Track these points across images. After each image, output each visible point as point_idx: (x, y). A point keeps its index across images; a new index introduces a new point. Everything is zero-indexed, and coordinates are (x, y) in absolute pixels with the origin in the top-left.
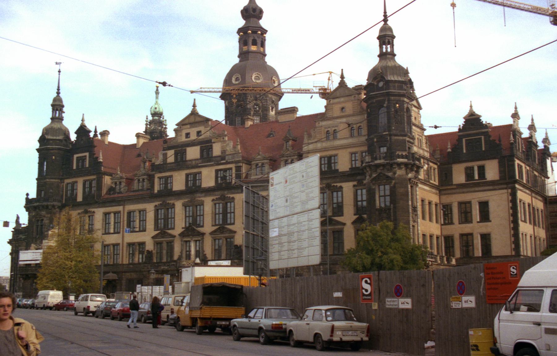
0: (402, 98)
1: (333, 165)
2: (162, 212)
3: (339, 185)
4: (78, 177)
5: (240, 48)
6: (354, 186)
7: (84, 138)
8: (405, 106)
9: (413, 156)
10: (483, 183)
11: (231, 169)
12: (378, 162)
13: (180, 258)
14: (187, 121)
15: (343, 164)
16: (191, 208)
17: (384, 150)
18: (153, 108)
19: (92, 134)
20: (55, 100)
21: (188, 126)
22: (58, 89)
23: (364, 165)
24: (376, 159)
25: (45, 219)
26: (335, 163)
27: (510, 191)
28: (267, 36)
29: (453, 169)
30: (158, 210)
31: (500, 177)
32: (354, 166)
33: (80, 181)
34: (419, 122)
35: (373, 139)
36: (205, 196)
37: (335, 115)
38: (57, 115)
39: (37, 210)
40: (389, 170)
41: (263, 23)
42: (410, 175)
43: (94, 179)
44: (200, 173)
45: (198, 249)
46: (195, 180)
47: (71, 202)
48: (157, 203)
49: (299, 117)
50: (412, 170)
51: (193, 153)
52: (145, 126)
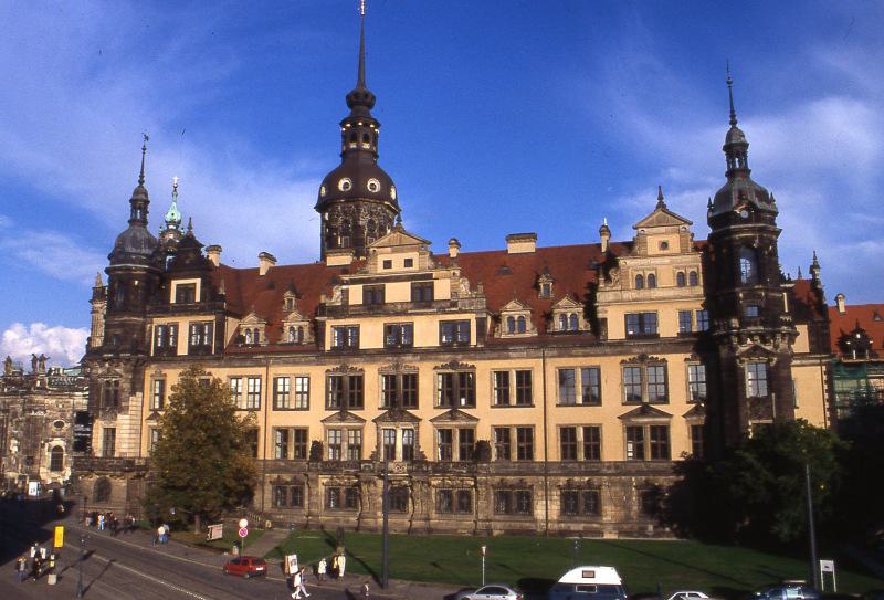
3: (660, 357)
4: (180, 316)
6: (686, 360)
11: (468, 322)
13: (375, 456)
20: (137, 192)
22: (142, 176)
25: (122, 381)
27: (824, 368)
31: (811, 350)
33: (184, 324)
36: (422, 360)
37: (649, 253)
41: (373, 113)
43: (210, 323)
45: (406, 442)
48: (330, 367)
51: (397, 293)
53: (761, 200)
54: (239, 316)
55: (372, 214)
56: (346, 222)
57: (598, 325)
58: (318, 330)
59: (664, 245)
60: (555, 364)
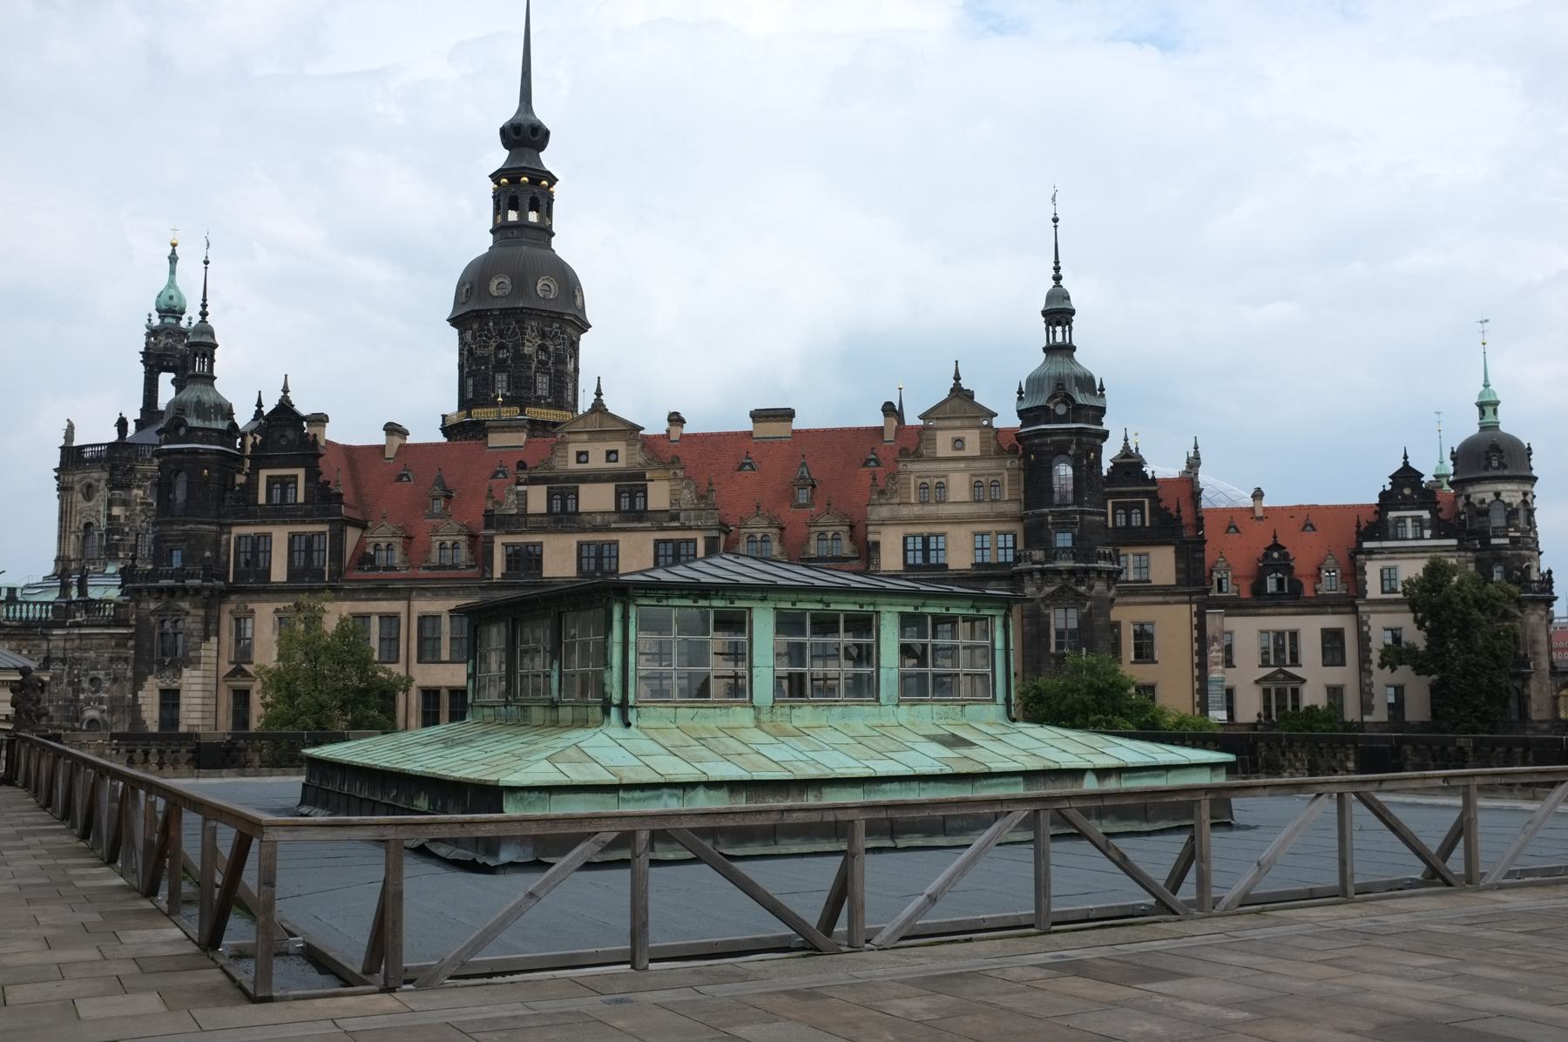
1: (933, 554)
4: (273, 523)
15: (959, 553)
17: (1064, 540)
18: (165, 298)
21: (585, 437)
23: (1022, 566)
27: (1195, 608)
28: (555, 189)
32: (979, 560)
33: (280, 536)
39: (164, 597)
40: (1080, 582)
42: (1113, 592)
46: (599, 556)
47: (253, 580)
49: (799, 432)
51: (596, 498)
52: (144, 339)
53: (1082, 391)
55: (543, 335)
56: (500, 347)
59: (958, 443)
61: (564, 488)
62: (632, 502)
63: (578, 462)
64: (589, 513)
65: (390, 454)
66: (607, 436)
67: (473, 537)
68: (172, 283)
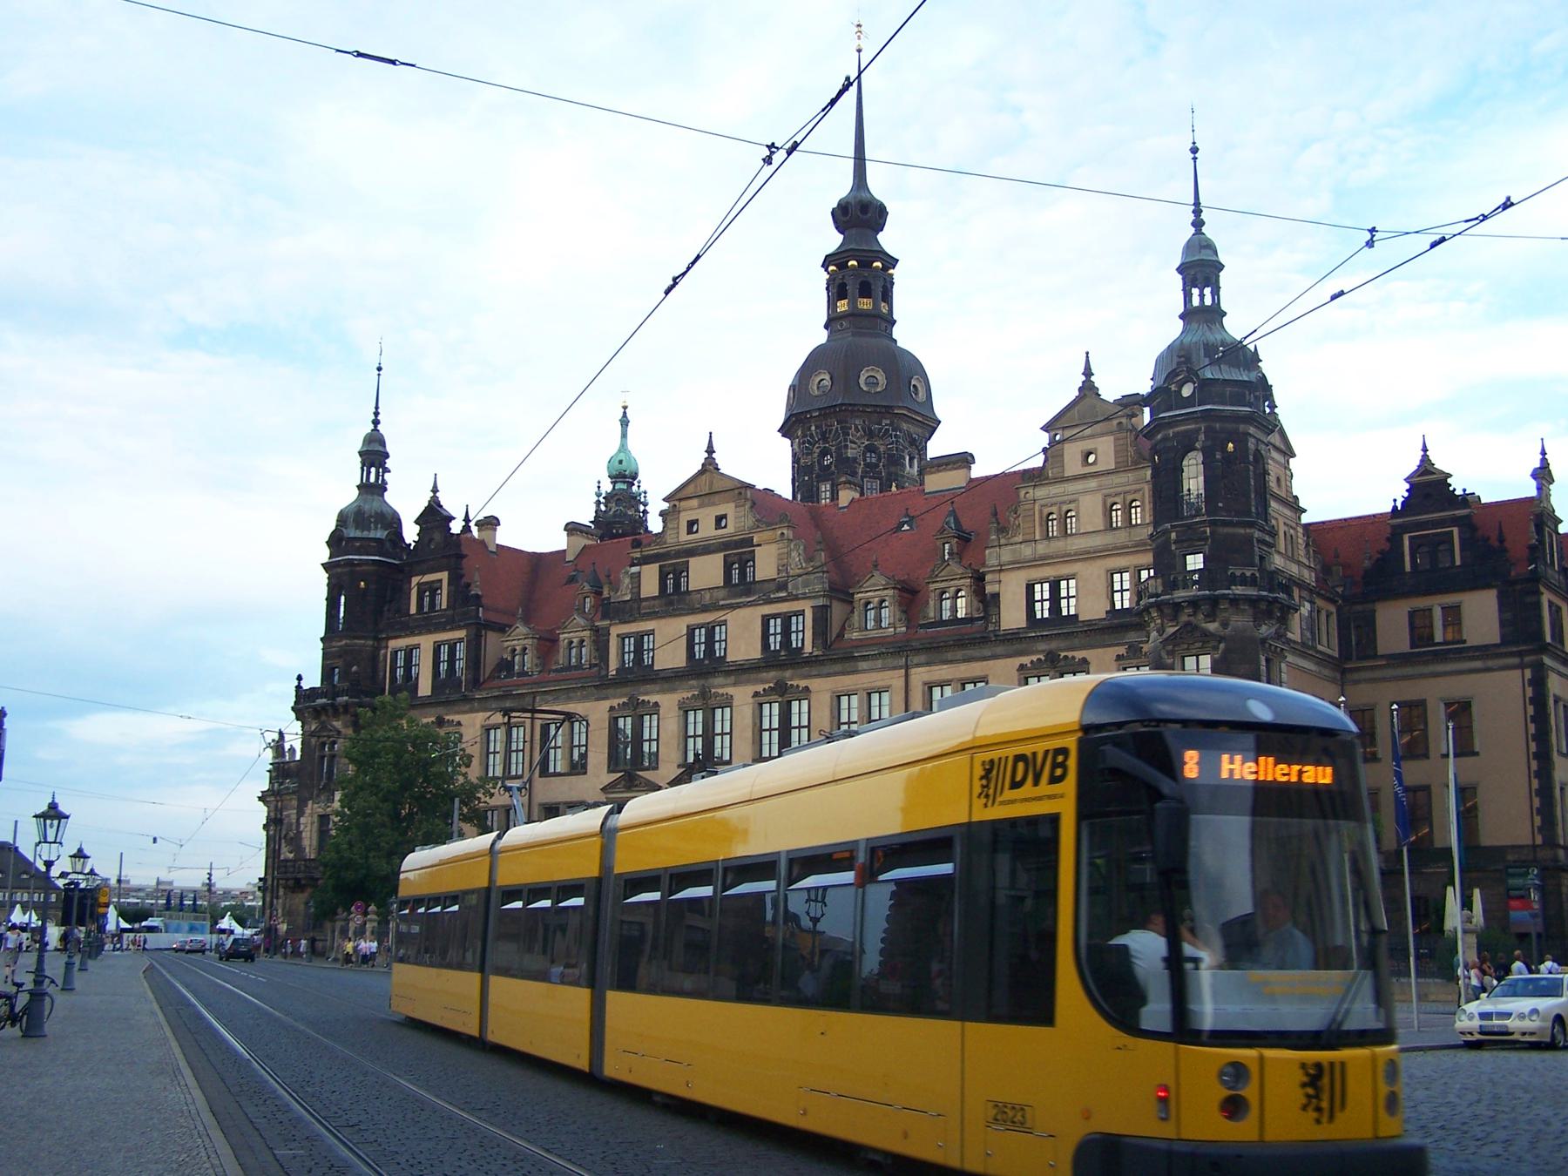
0: (1242, 427)
1: (1064, 603)
2: (626, 724)
3: (1079, 655)
4: (420, 634)
5: (831, 304)
7: (437, 536)
8: (1251, 444)
9: (1273, 580)
10: (1458, 652)
11: (802, 613)
12: (1180, 595)
14: (690, 490)
16: (700, 714)
17: (1195, 562)
19: (456, 527)
21: (695, 502)
22: (376, 414)
24: (1171, 586)
26: (1068, 597)
27: (1528, 673)
28: (896, 273)
29: (1377, 615)
30: (616, 719)
31: (1503, 636)
33: (426, 642)
34: (1289, 489)
35: (1167, 532)
36: (735, 684)
38: (372, 479)
39: (323, 718)
40: (1211, 617)
41: (888, 239)
42: (1265, 630)
44: (725, 623)
50: (1269, 614)
51: (706, 573)
54: (502, 629)
55: (870, 434)
57: (988, 603)
58: (600, 641)
60: (920, 675)
61: (674, 565)
62: (743, 574)
63: (690, 532)
64: (698, 591)
65: (570, 557)
66: (717, 497)
67: (596, 630)
68: (623, 447)
